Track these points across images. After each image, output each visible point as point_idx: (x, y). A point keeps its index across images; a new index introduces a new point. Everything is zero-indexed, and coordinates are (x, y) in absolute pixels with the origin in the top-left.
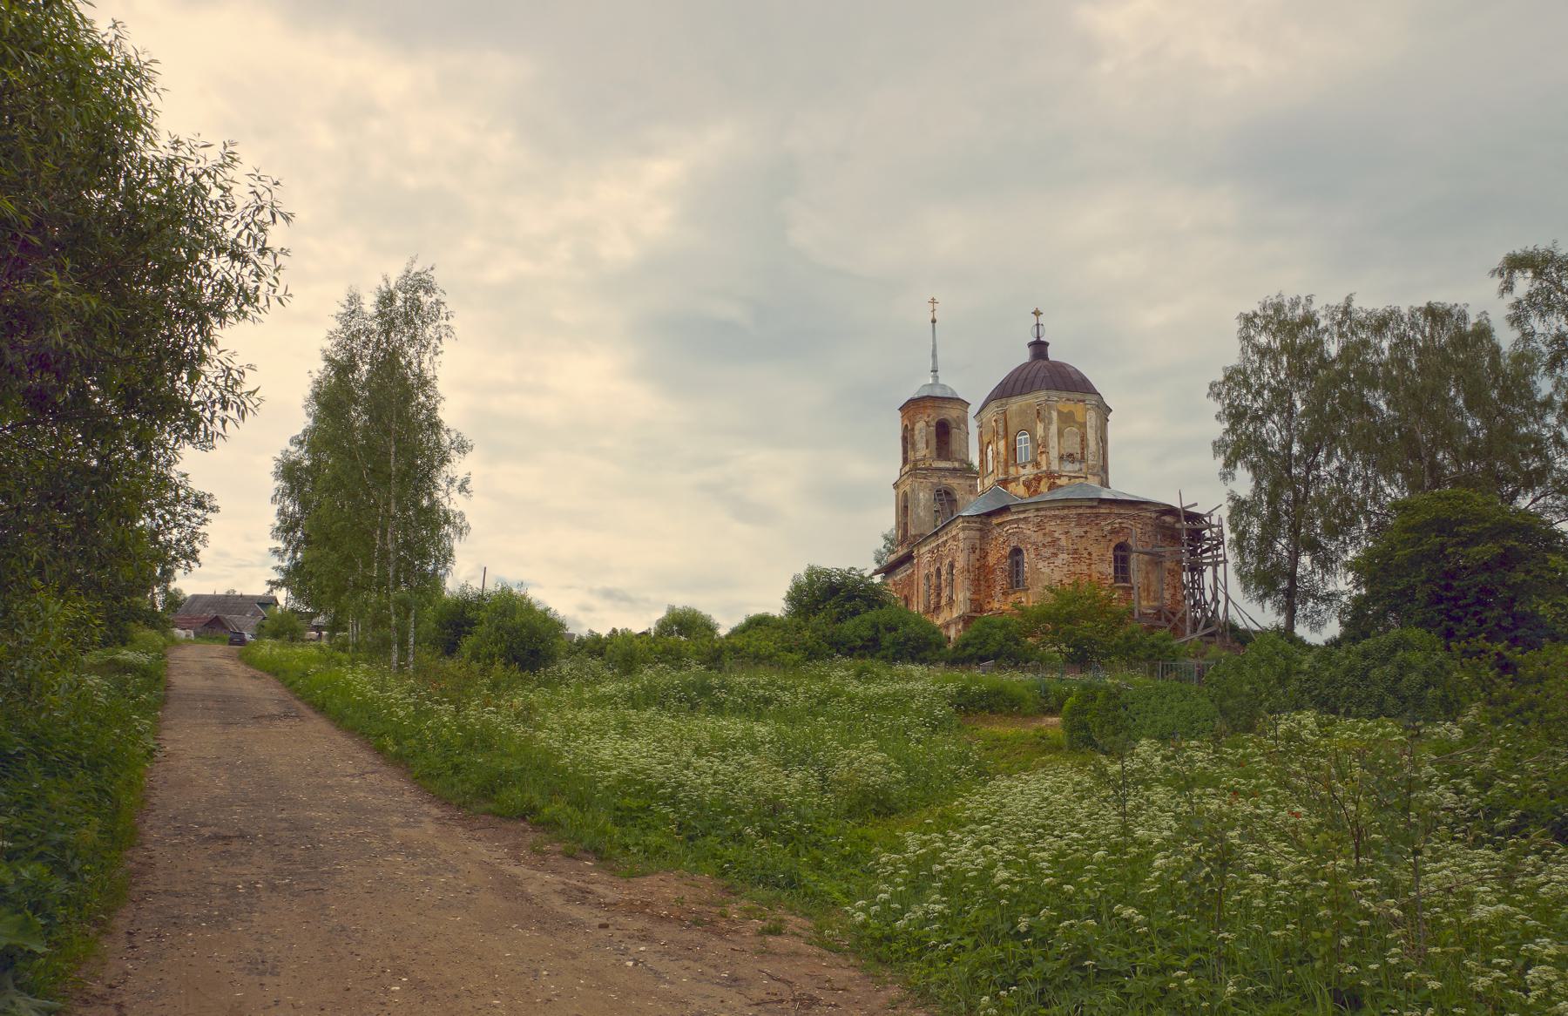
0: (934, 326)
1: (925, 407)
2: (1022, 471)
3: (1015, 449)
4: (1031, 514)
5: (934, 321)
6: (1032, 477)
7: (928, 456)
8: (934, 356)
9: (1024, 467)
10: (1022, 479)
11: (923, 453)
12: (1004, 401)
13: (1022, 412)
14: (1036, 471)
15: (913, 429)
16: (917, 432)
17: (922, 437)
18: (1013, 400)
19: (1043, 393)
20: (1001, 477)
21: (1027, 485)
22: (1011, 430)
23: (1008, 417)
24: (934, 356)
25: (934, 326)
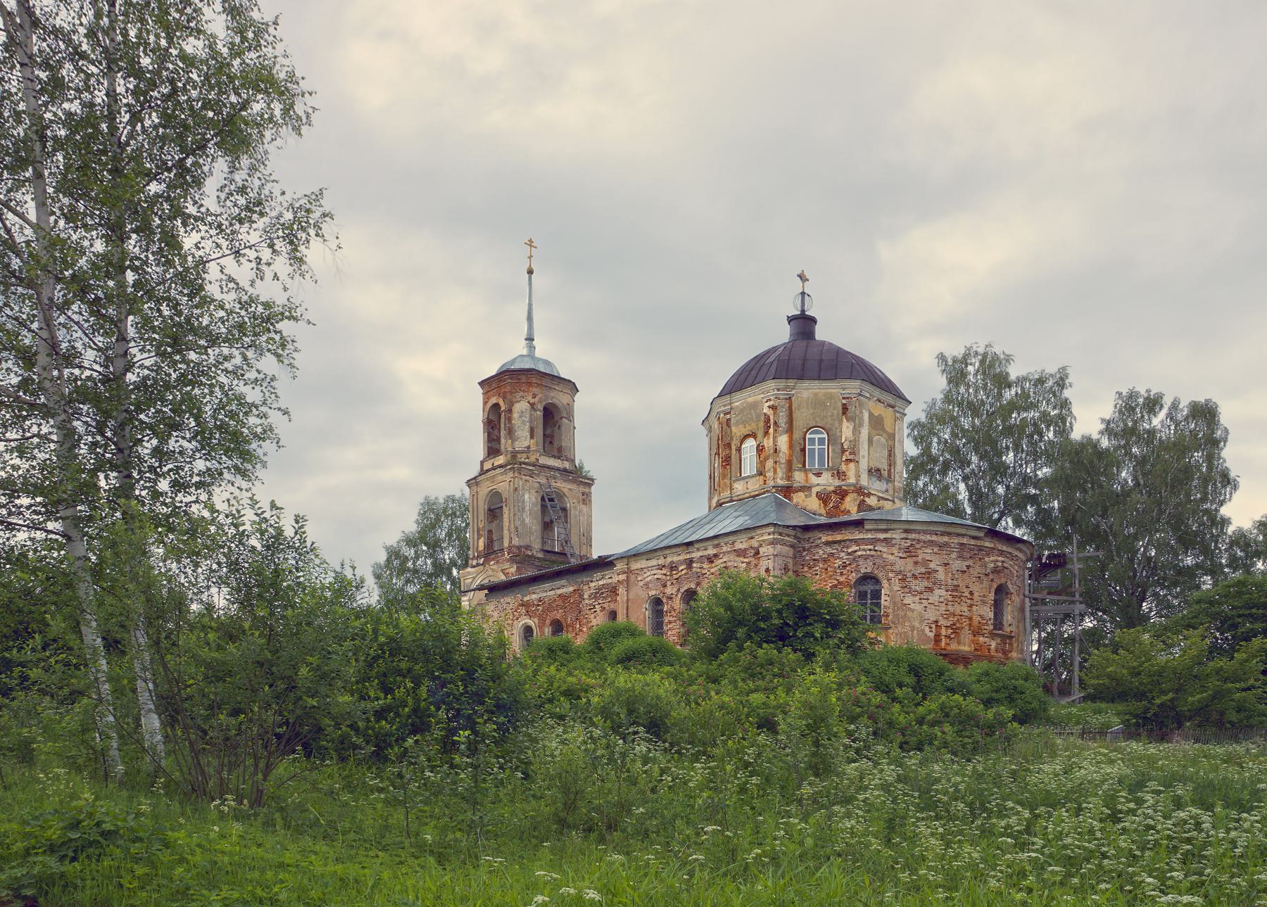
0: (530, 279)
1: (530, 384)
3: (803, 450)
5: (530, 272)
8: (530, 318)
11: (526, 443)
12: (791, 383)
13: (818, 403)
15: (510, 411)
16: (515, 415)
18: (806, 384)
20: (780, 482)
23: (794, 406)
24: (530, 318)
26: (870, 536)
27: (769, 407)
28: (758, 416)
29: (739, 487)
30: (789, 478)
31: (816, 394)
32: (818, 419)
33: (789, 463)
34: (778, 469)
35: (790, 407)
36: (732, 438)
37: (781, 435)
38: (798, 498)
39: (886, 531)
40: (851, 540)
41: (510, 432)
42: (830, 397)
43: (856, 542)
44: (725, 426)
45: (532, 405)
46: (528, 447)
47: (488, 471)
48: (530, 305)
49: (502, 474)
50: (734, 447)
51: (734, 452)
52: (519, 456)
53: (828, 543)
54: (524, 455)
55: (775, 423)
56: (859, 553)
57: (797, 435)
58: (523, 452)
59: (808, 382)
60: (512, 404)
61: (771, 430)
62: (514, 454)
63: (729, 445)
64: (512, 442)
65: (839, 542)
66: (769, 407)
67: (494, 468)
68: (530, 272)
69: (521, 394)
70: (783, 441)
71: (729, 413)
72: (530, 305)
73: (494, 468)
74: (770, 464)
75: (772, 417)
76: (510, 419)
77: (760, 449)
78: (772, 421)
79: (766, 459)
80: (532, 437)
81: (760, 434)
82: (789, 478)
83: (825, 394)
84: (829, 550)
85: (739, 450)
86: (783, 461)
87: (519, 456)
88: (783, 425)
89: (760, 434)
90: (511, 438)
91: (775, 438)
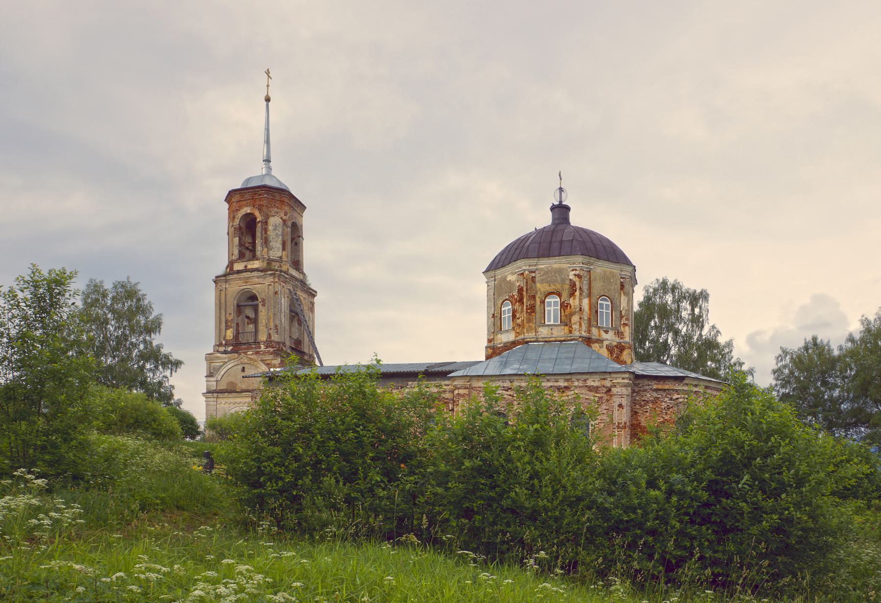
0: (267, 106)
1: (282, 202)
2: (604, 336)
3: (597, 312)
4: (701, 389)
5: (268, 100)
6: (615, 344)
7: (284, 259)
8: (268, 142)
9: (606, 332)
10: (605, 343)
11: (279, 254)
12: (592, 260)
13: (606, 278)
14: (618, 340)
15: (266, 223)
16: (270, 228)
17: (277, 235)
18: (600, 263)
19: (579, 259)
20: (584, 334)
21: (610, 349)
22: (595, 291)
23: (592, 277)
24: (268, 142)
25: (267, 106)
26: (686, 388)
27: (575, 275)
28: (563, 281)
29: (544, 332)
30: (589, 331)
31: (605, 272)
32: (606, 290)
33: (589, 320)
34: (583, 324)
35: (590, 278)
36: (536, 293)
37: (585, 298)
38: (595, 346)
39: (696, 386)
40: (673, 390)
41: (266, 242)
42: (613, 275)
43: (677, 391)
44: (530, 282)
45: (284, 221)
46: (281, 257)
47: (239, 272)
48: (268, 130)
49: (258, 277)
50: (538, 300)
51: (538, 303)
52: (273, 264)
53: (657, 390)
54: (278, 264)
55: (580, 288)
56: (681, 400)
57: (593, 301)
58: (277, 261)
59: (602, 261)
60: (267, 217)
61: (577, 293)
62: (270, 261)
63: (534, 297)
64: (268, 251)
65: (665, 390)
66: (575, 275)
67: (246, 270)
68: (268, 100)
69: (276, 209)
70: (586, 302)
71: (534, 272)
72: (268, 130)
73: (246, 270)
74: (575, 318)
75: (578, 284)
76: (266, 230)
77: (564, 306)
78: (578, 286)
79: (572, 314)
80: (284, 249)
81: (565, 295)
82: (589, 331)
83: (611, 272)
84: (655, 394)
85: (543, 302)
86: (586, 318)
87: (273, 264)
88: (585, 291)
89: (565, 295)
90: (266, 247)
91: (580, 299)
